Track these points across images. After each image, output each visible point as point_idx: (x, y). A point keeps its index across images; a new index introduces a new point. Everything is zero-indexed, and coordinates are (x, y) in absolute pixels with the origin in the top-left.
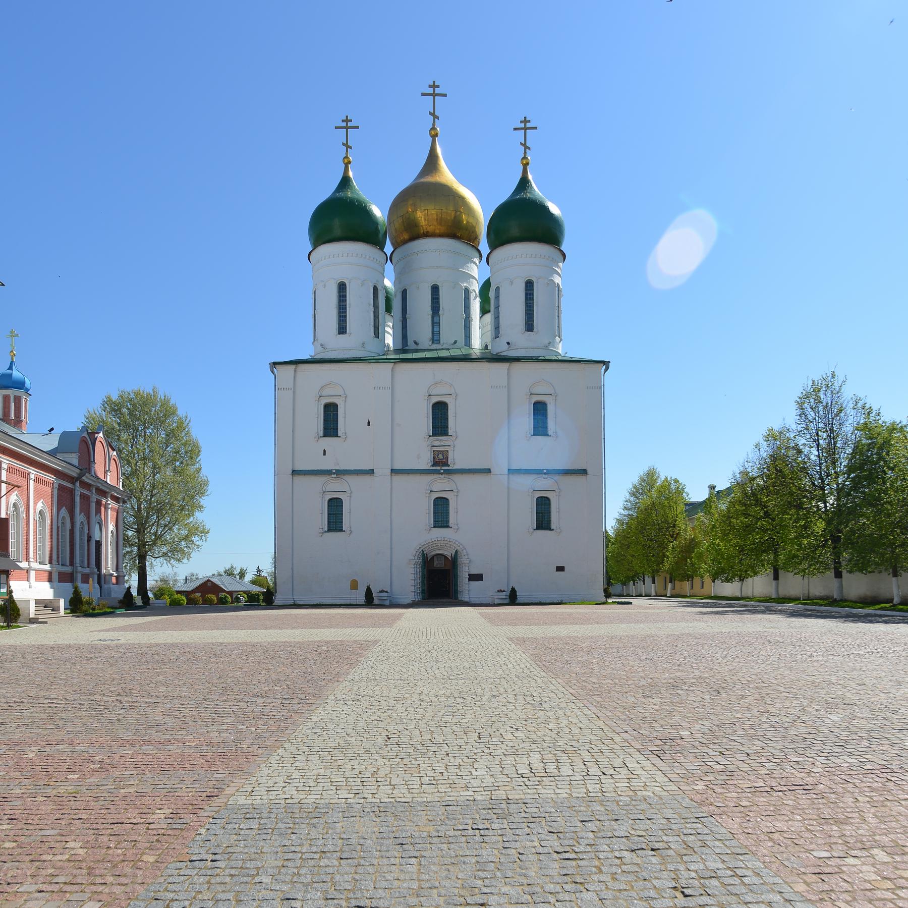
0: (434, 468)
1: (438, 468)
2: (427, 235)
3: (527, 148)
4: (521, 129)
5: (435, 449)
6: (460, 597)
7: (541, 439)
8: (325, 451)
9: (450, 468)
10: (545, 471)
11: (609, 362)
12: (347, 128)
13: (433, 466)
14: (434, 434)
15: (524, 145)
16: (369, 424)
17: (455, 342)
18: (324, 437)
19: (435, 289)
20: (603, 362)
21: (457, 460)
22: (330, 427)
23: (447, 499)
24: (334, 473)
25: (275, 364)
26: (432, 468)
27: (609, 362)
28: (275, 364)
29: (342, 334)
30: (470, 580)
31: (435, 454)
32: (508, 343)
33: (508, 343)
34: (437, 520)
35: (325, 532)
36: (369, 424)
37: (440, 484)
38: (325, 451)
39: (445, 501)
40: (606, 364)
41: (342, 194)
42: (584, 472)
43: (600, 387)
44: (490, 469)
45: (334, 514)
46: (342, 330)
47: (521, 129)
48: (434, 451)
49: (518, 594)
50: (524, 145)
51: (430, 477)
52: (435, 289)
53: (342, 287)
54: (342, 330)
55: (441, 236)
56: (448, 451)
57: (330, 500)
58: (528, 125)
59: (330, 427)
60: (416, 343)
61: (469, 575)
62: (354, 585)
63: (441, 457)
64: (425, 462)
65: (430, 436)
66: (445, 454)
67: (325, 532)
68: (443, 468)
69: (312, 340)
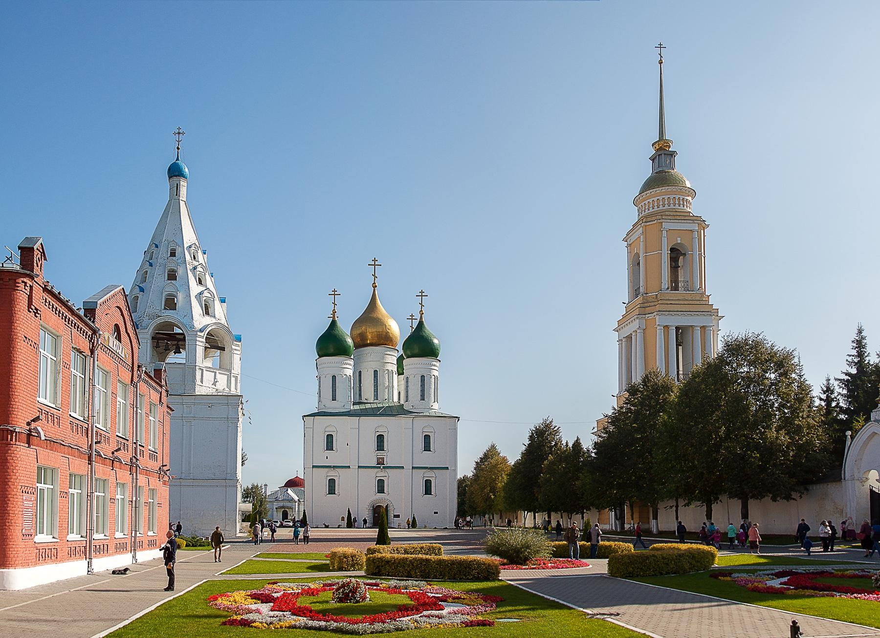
2: (371, 345)
3: (422, 306)
4: (420, 296)
5: (378, 457)
15: (421, 304)
20: (457, 417)
21: (388, 462)
22: (330, 446)
28: (305, 416)
37: (381, 474)
40: (458, 418)
46: (334, 399)
47: (420, 296)
50: (421, 304)
51: (376, 470)
54: (334, 399)
59: (330, 446)
60: (366, 399)
64: (374, 463)
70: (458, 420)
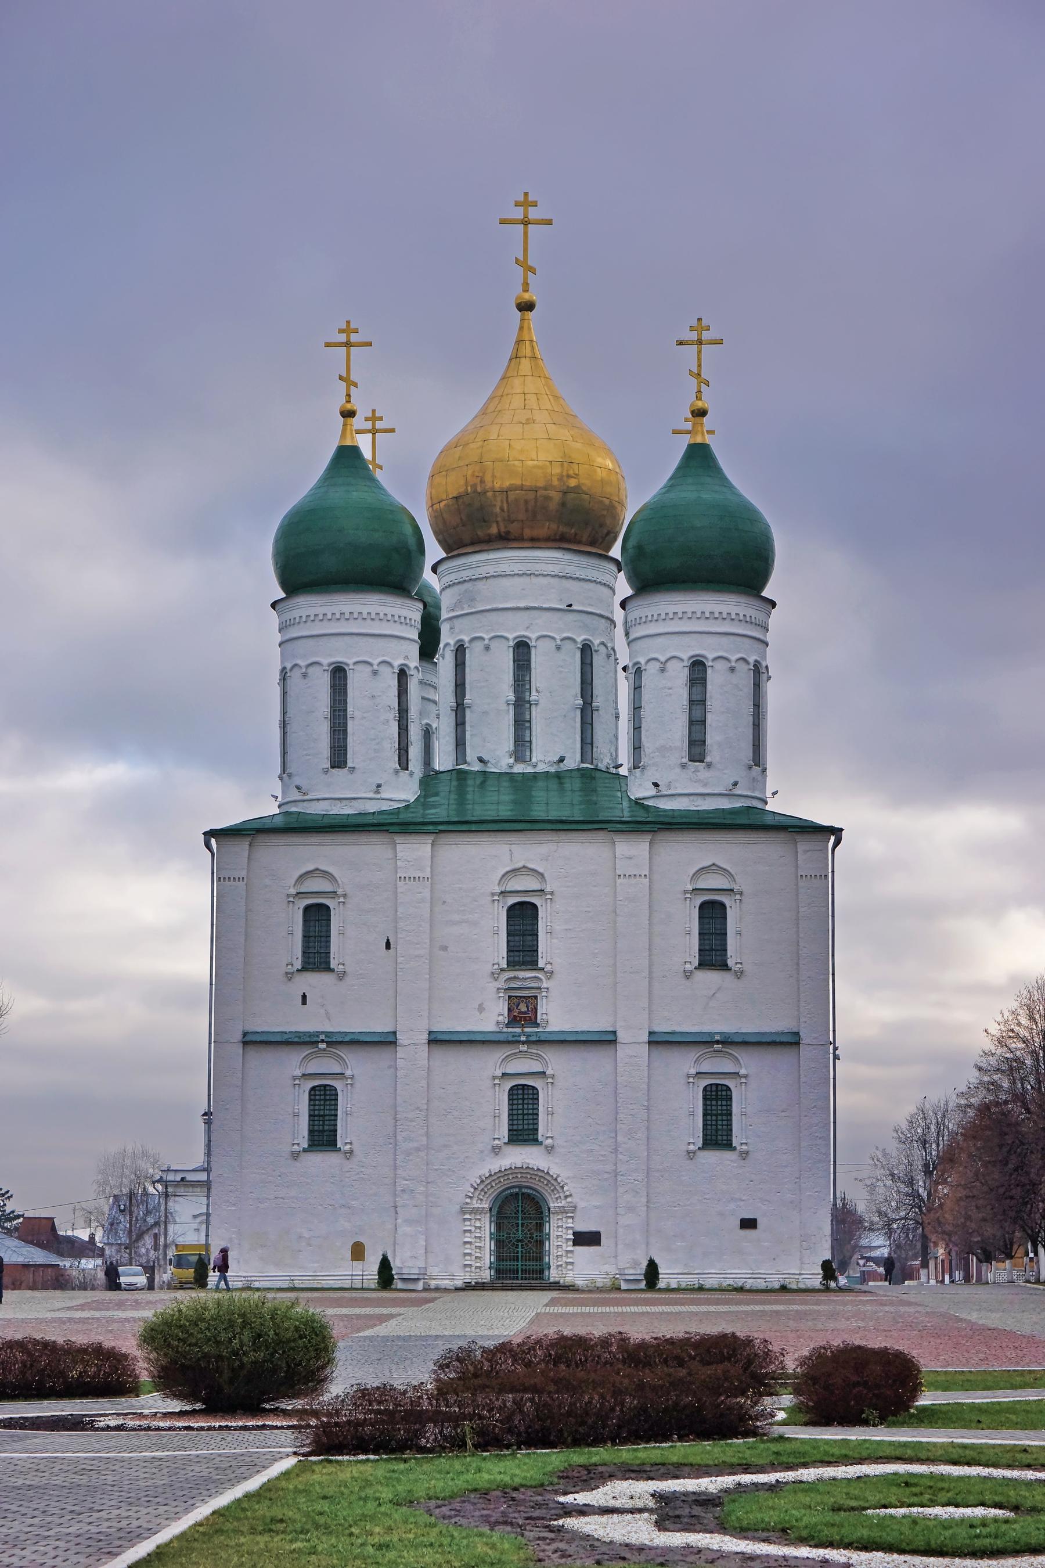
0: (510, 1030)
1: (518, 1030)
6: (553, 1275)
7: (712, 978)
8: (304, 997)
9: (540, 1029)
10: (718, 1038)
11: (842, 830)
12: (348, 344)
13: (507, 1026)
14: (512, 964)
16: (388, 945)
17: (561, 760)
18: (304, 969)
19: (522, 649)
23: (534, 1088)
24: (323, 1041)
25: (210, 834)
26: (505, 1030)
27: (842, 830)
29: (339, 767)
30: (576, 1243)
31: (513, 1002)
32: (656, 785)
33: (656, 785)
34: (515, 1127)
35: (305, 1150)
36: (388, 945)
38: (304, 997)
39: (531, 1092)
40: (836, 832)
41: (337, 495)
42: (791, 1042)
43: (826, 876)
44: (614, 1032)
45: (319, 1116)
46: (339, 758)
48: (510, 997)
49: (660, 1271)
52: (522, 649)
53: (339, 674)
54: (339, 758)
55: (535, 542)
56: (536, 997)
57: (313, 1089)
58: (706, 336)
60: (481, 760)
61: (574, 1234)
62: (358, 1252)
63: (523, 1008)
65: (502, 970)
66: (532, 1001)
67: (305, 1150)
68: (526, 1030)
69: (278, 771)
70: (837, 842)
